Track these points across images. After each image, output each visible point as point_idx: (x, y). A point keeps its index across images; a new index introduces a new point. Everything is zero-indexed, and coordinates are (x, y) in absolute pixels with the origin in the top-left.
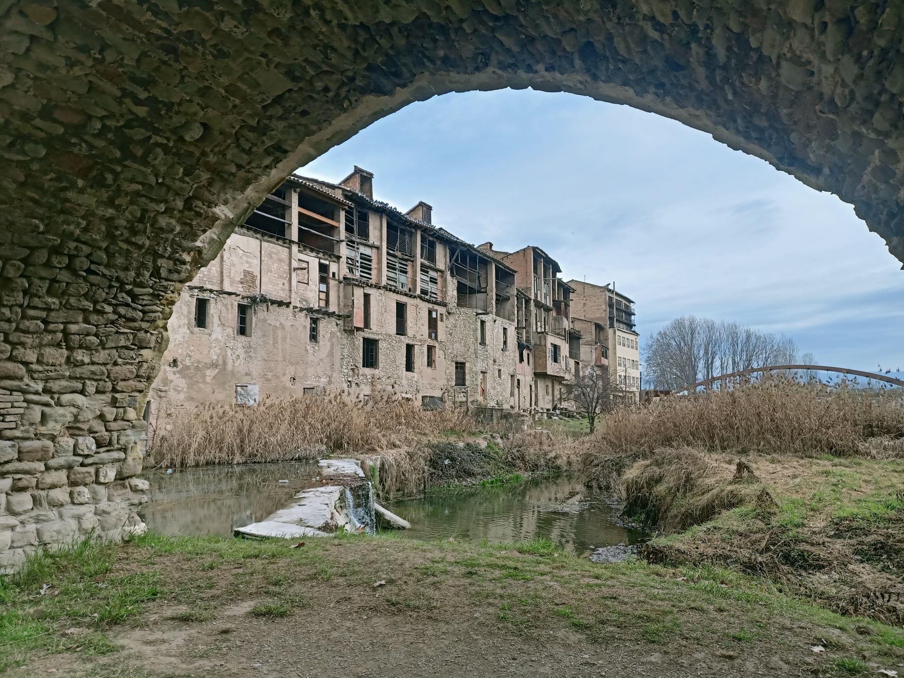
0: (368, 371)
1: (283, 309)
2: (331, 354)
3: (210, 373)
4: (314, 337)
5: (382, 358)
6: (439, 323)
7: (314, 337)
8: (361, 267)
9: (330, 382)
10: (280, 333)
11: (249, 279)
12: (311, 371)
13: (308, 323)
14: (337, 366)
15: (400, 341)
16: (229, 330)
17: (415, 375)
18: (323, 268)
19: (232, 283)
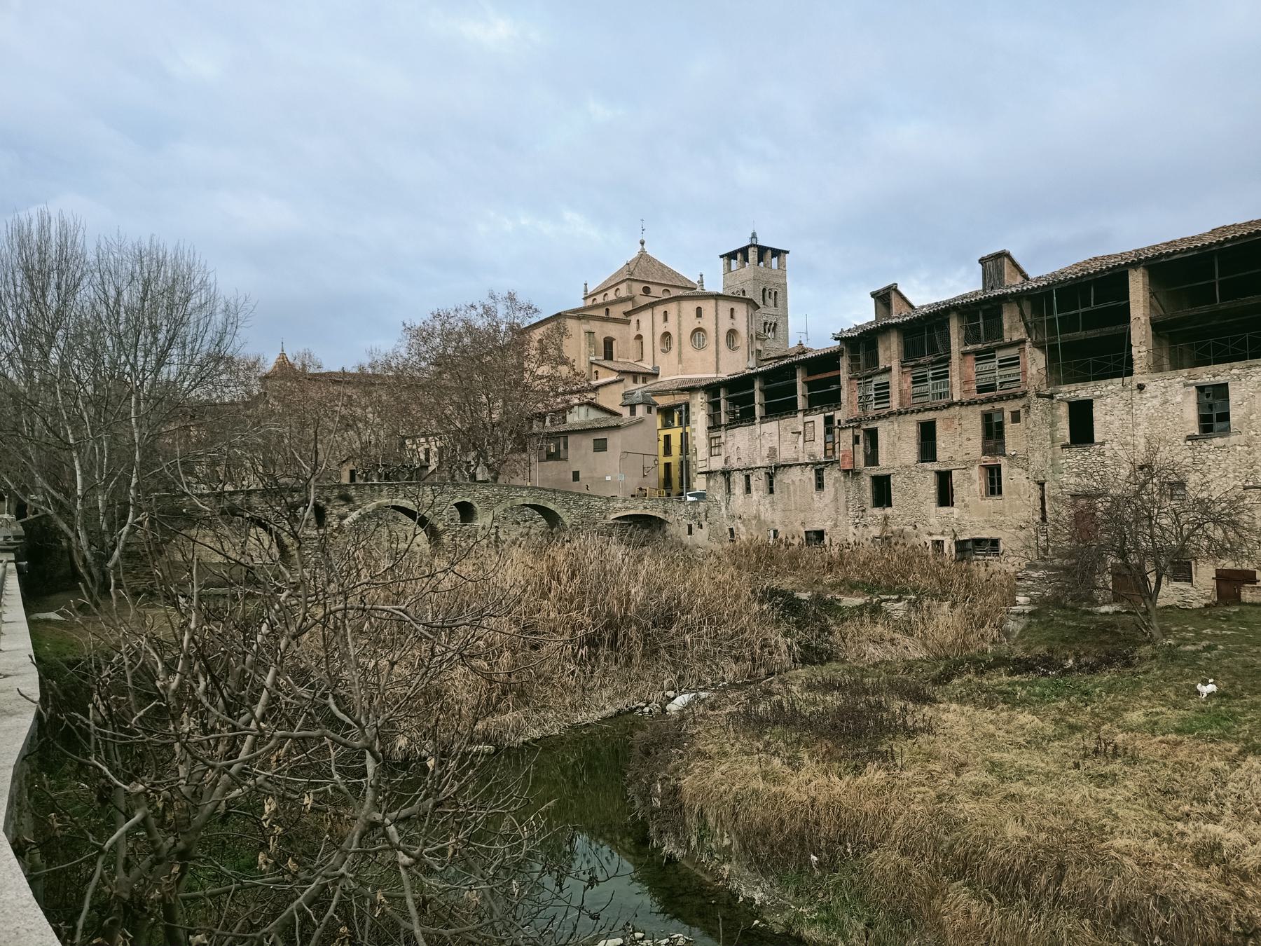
0: (878, 512)
1: (793, 469)
2: (836, 499)
3: (754, 522)
4: (820, 486)
5: (895, 495)
6: (1008, 426)
7: (820, 486)
8: (876, 399)
9: (836, 525)
10: (792, 488)
11: (773, 452)
12: (817, 516)
13: (812, 475)
14: (842, 509)
15: (925, 470)
16: (761, 492)
17: (955, 511)
18: (829, 421)
19: (763, 459)
